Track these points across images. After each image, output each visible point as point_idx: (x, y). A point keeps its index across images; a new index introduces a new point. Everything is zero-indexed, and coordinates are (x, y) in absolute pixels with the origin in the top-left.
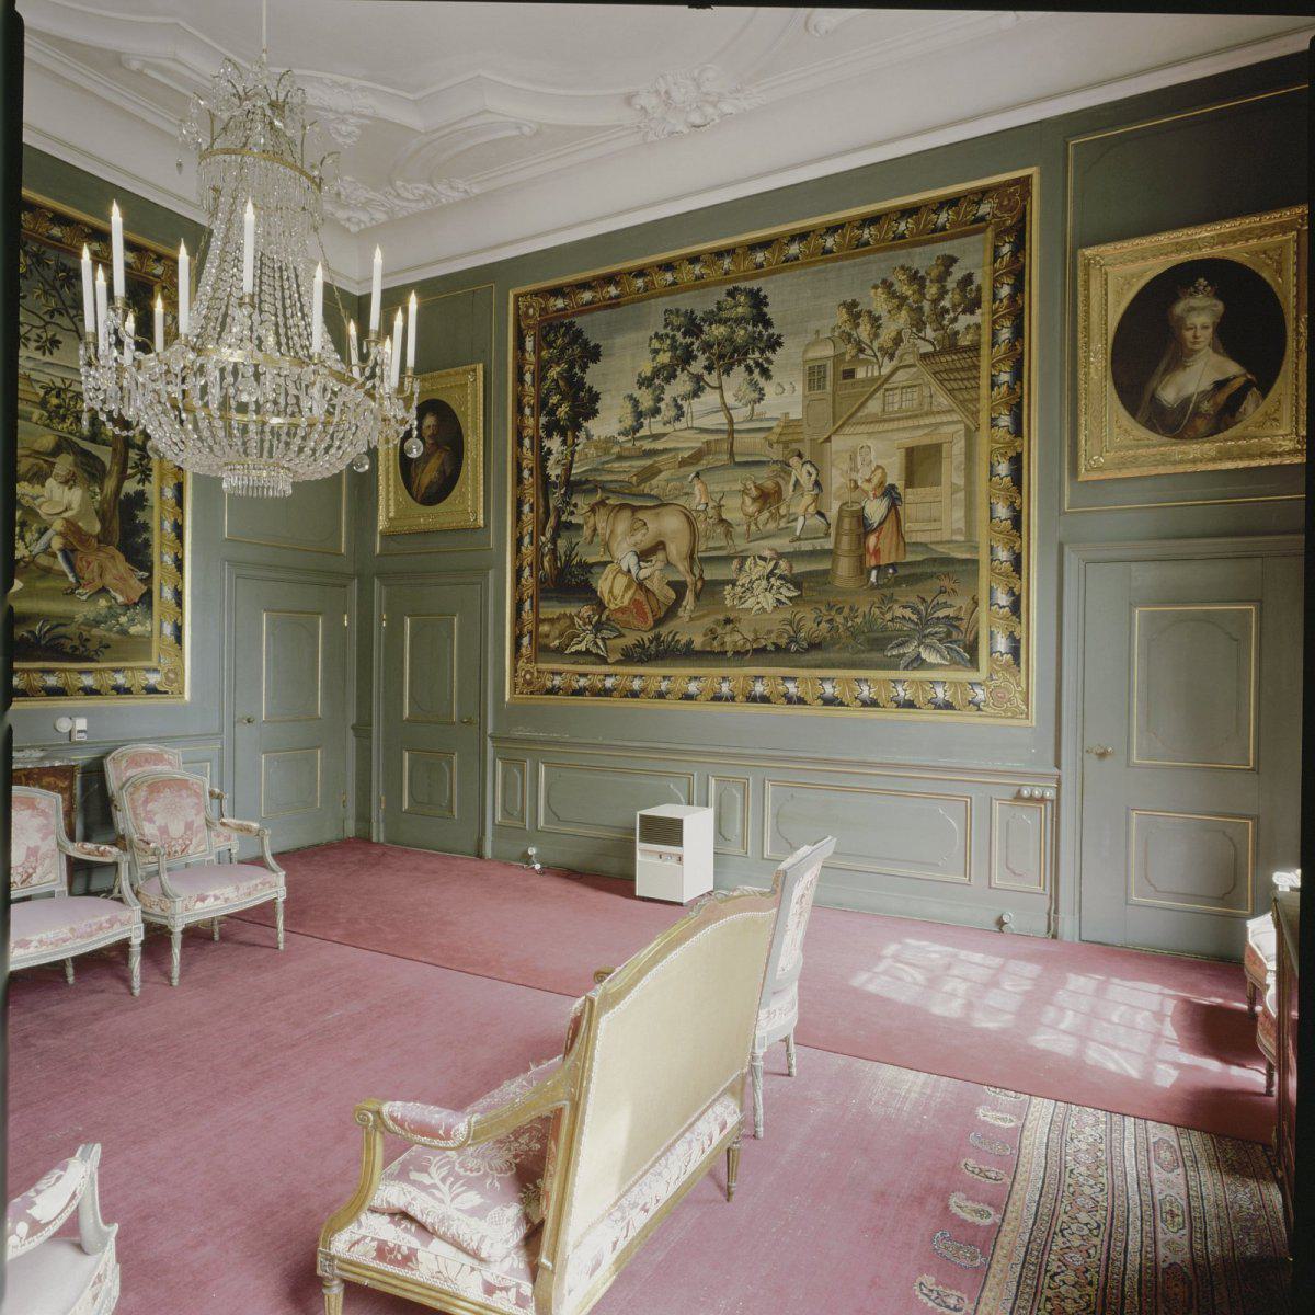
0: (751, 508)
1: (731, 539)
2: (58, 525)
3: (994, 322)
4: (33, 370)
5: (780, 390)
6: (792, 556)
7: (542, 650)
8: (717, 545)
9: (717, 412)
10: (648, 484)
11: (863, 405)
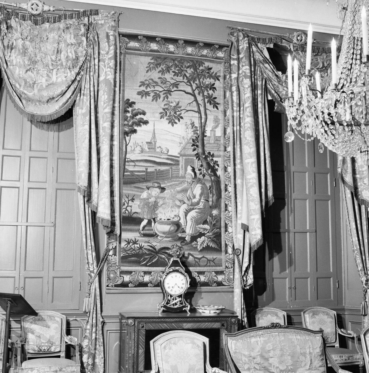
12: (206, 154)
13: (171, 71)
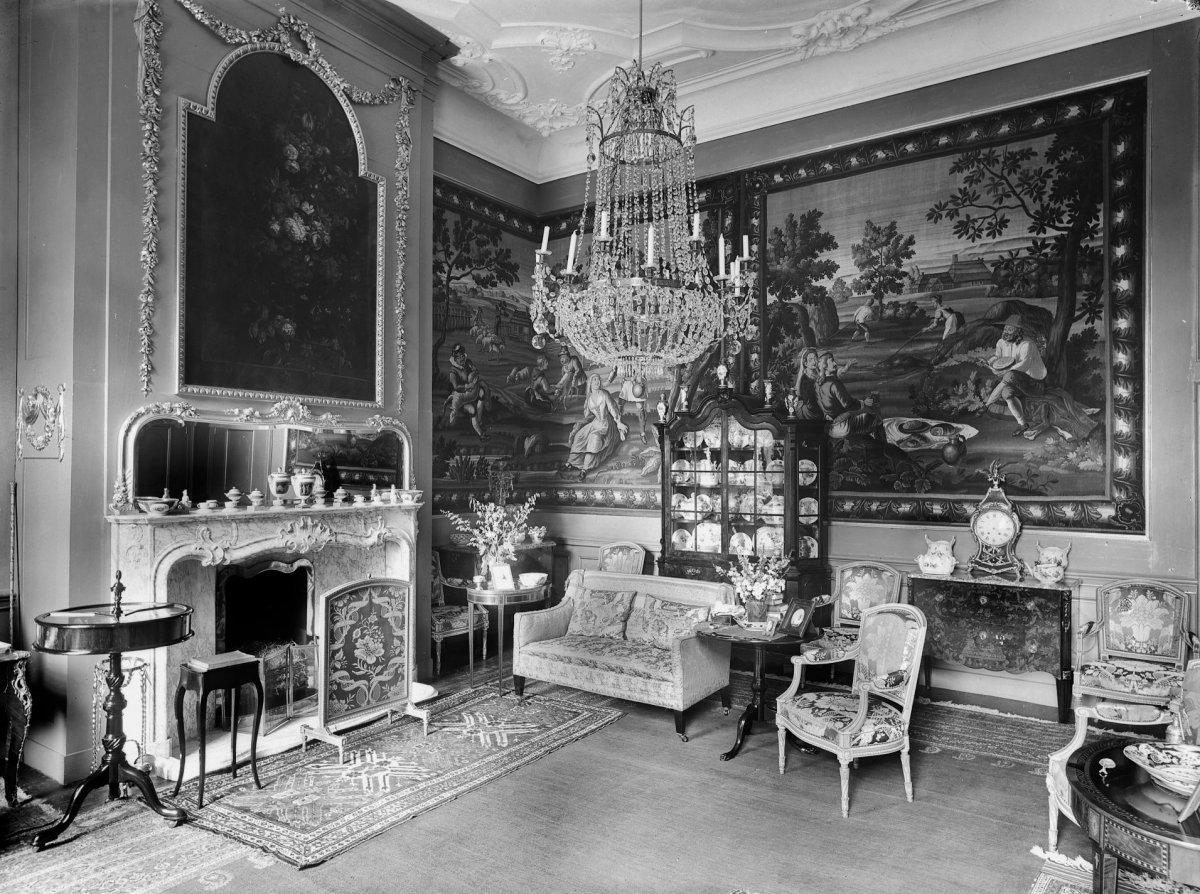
2: (1007, 377)
4: (986, 253)
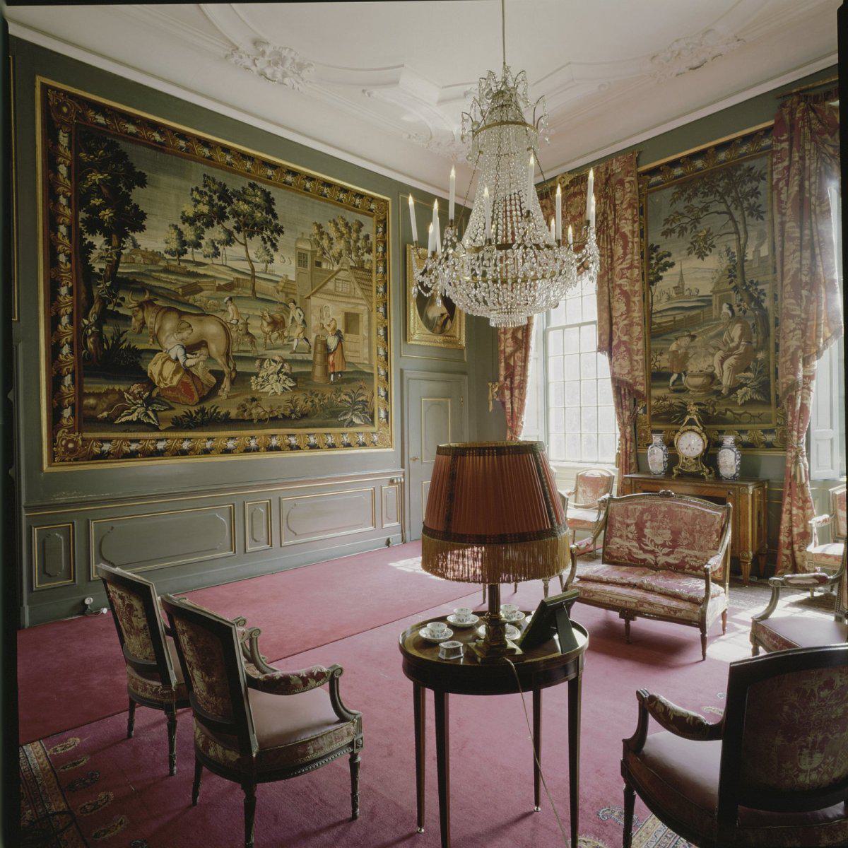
0: (267, 329)
1: (255, 347)
3: (377, 262)
5: (282, 260)
6: (293, 362)
7: (87, 420)
8: (245, 349)
9: (243, 260)
10: (192, 297)
11: (325, 283)
12: (748, 283)
13: (699, 194)
